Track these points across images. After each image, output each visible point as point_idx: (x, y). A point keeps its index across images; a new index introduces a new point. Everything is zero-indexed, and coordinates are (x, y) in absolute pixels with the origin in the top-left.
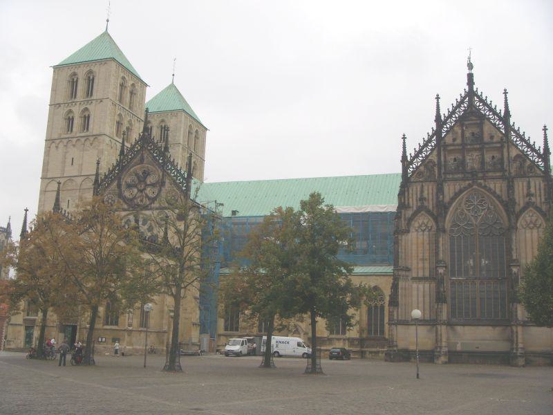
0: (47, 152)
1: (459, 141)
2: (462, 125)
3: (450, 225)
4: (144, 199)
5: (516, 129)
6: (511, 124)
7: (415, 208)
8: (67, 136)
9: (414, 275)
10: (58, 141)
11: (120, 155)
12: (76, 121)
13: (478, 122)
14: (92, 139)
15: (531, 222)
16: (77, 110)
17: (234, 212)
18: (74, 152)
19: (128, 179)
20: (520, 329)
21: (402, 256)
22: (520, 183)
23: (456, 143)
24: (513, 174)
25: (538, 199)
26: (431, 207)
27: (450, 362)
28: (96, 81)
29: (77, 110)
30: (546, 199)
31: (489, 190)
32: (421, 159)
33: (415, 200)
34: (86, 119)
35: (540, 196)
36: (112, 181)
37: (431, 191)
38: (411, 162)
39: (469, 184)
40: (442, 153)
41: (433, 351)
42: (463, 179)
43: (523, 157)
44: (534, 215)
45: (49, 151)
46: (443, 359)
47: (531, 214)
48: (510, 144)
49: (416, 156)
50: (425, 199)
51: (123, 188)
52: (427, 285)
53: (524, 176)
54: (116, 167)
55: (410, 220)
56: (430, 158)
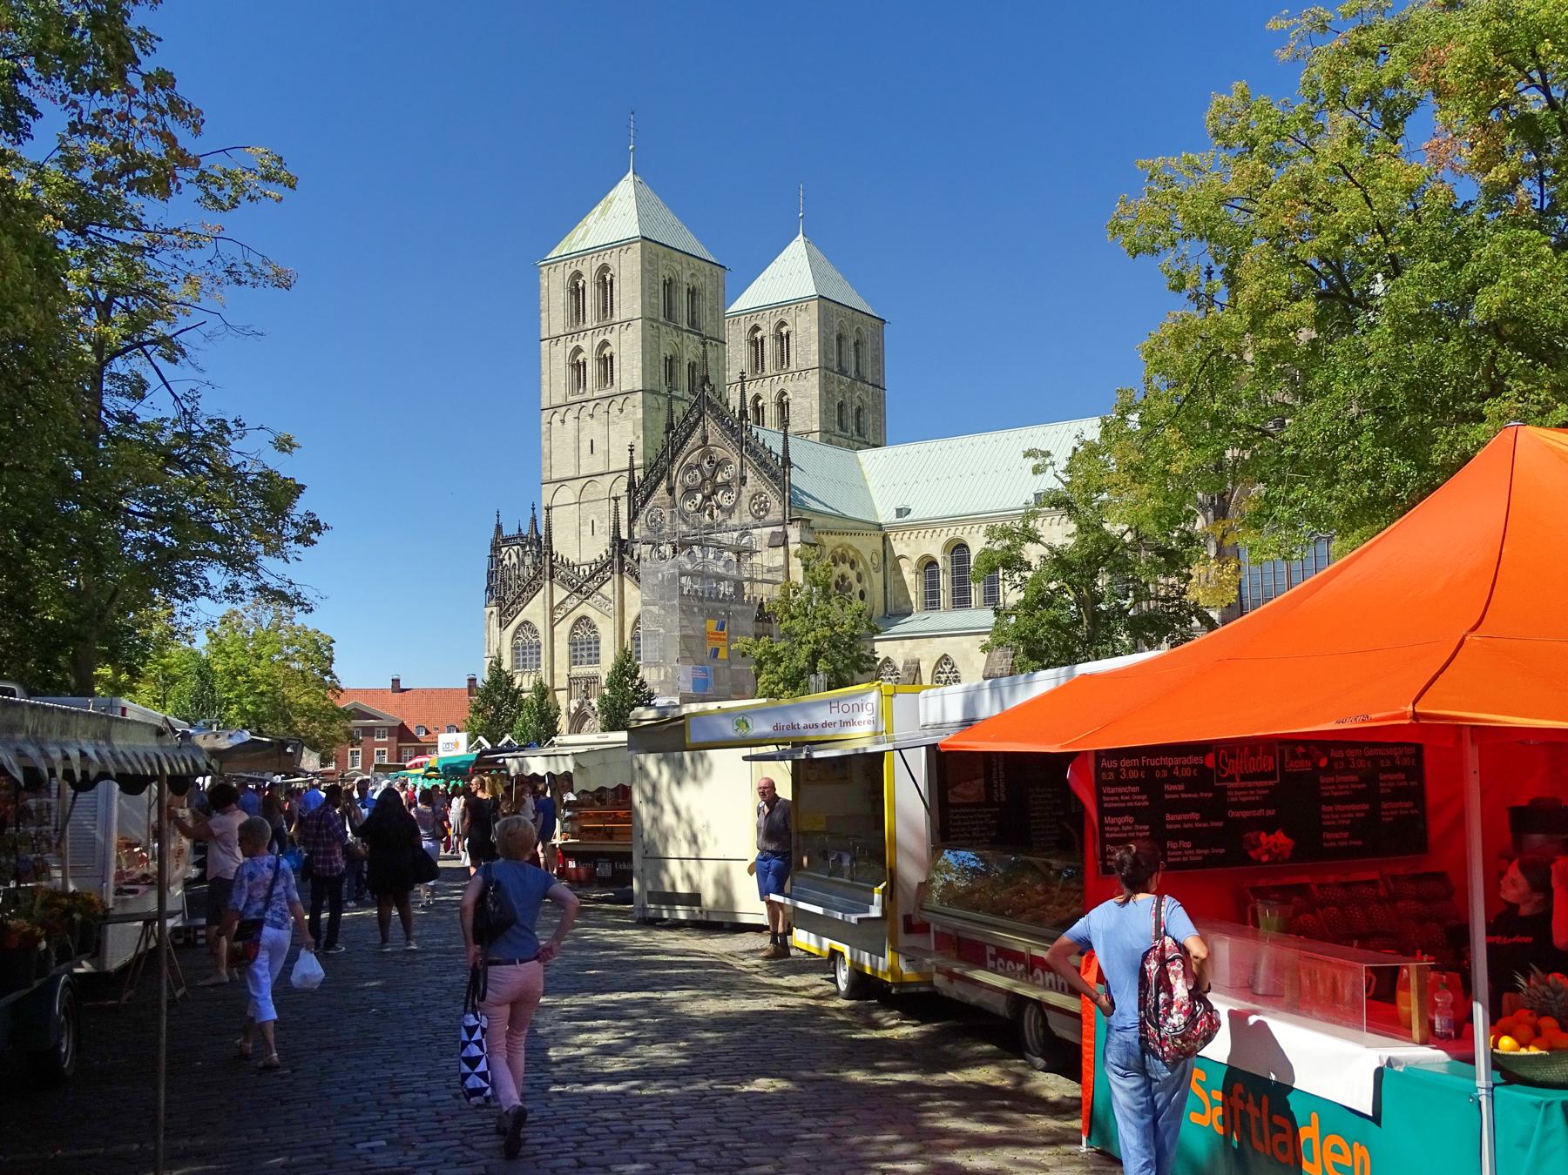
4: (715, 512)
10: (564, 409)
11: (667, 432)
12: (589, 369)
14: (620, 399)
17: (901, 512)
18: (593, 429)
28: (616, 285)
29: (588, 344)
34: (606, 363)
36: (658, 482)
51: (678, 493)
54: (662, 456)
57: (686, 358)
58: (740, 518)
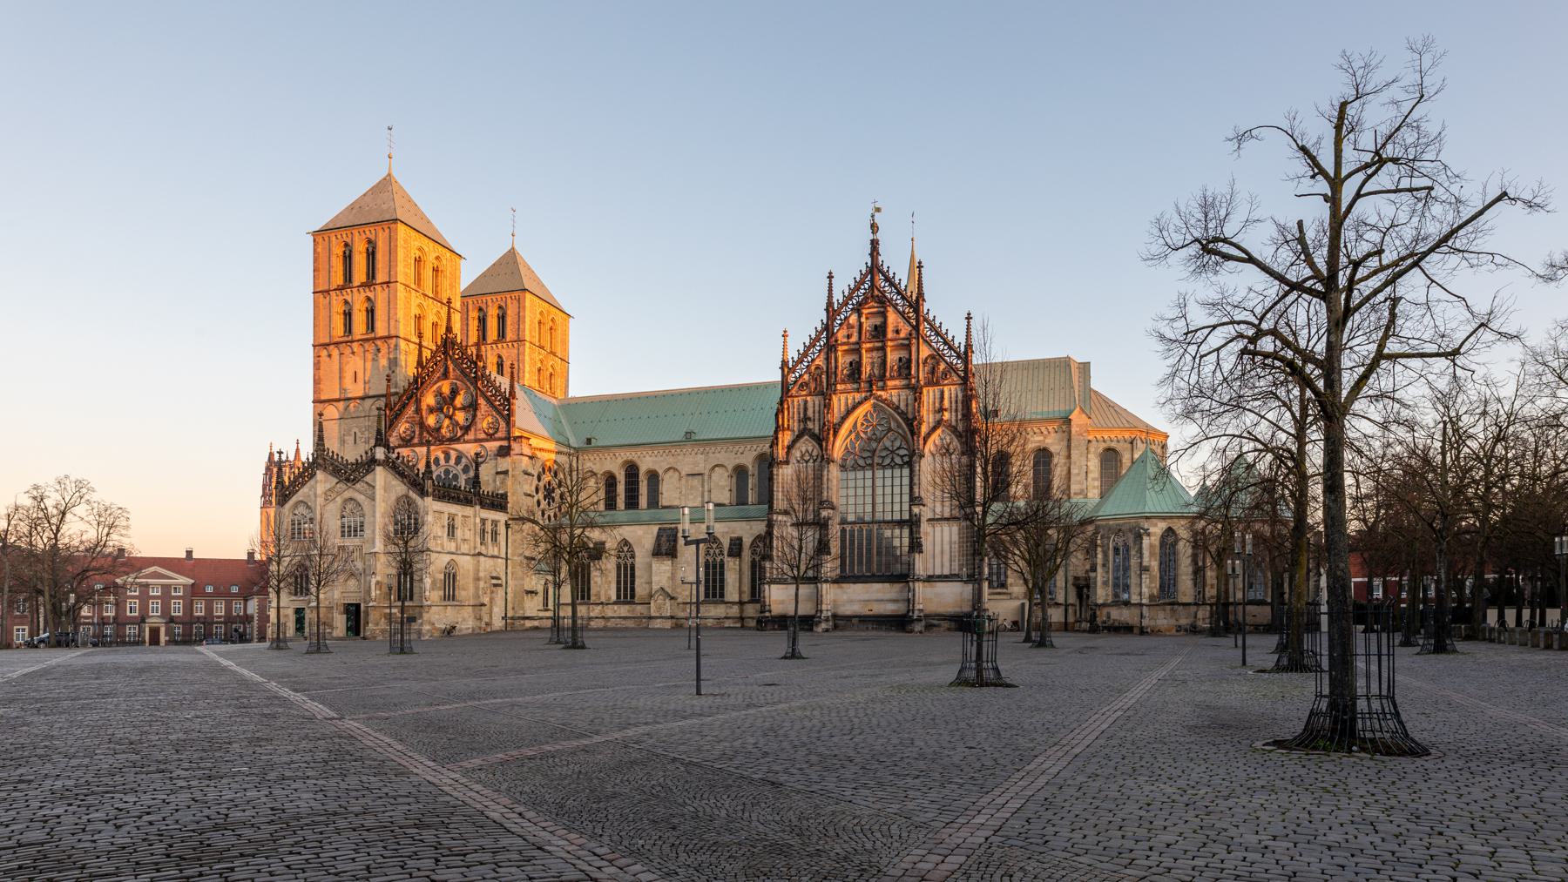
0: (317, 366)
1: (854, 339)
2: (860, 317)
5: (931, 318)
6: (925, 311)
7: (796, 433)
8: (346, 339)
10: (332, 347)
14: (379, 342)
15: (943, 446)
16: (358, 301)
19: (429, 400)
20: (919, 587)
24: (922, 383)
25: (953, 414)
26: (817, 431)
27: (836, 627)
29: (358, 301)
30: (963, 415)
34: (371, 312)
35: (956, 411)
37: (817, 408)
38: (792, 370)
41: (813, 617)
42: (858, 390)
43: (937, 357)
45: (319, 362)
46: (824, 626)
48: (921, 340)
49: (800, 361)
50: (809, 419)
53: (937, 384)
55: (790, 448)
56: (817, 362)
57: (431, 318)
58: (475, 434)
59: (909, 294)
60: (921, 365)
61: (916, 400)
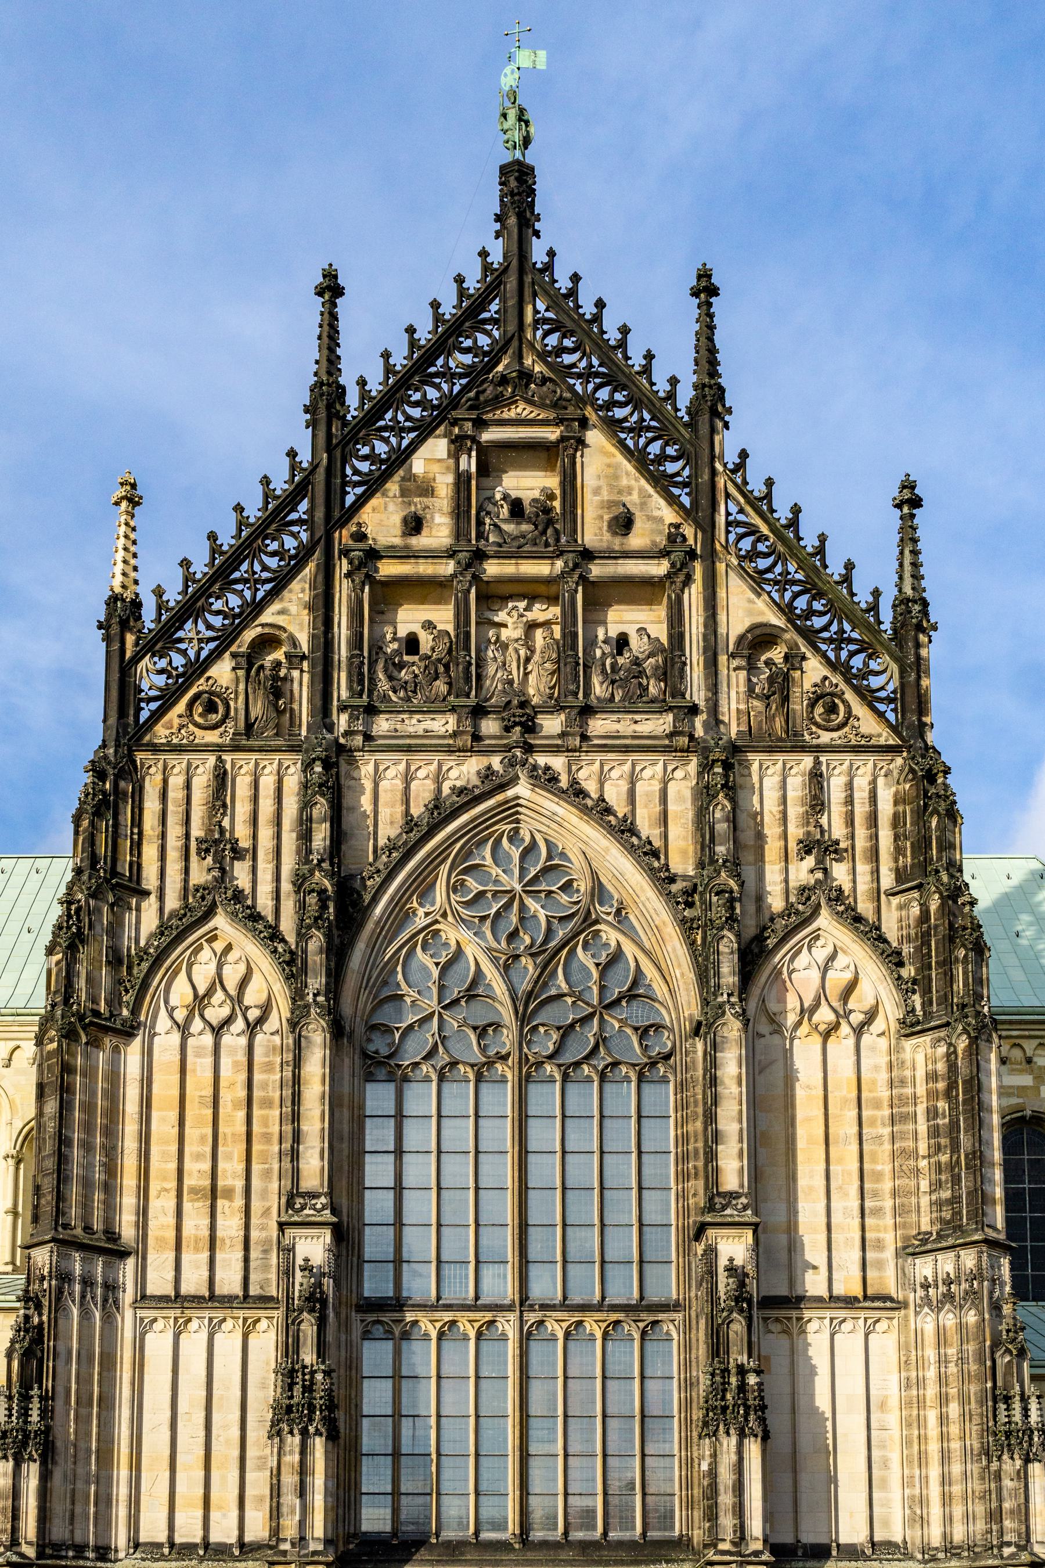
3: (365, 1001)
5: (757, 487)
7: (172, 903)
9: (159, 1282)
13: (552, 434)
21: (88, 1167)
22: (771, 783)
23: (421, 541)
25: (863, 869)
30: (900, 876)
31: (601, 811)
32: (217, 621)
33: (173, 855)
37: (266, 807)
39: (488, 773)
40: (343, 590)
44: (841, 960)
47: (821, 953)
52: (228, 1342)
56: (268, 616)
59: (662, 387)
60: (723, 659)
61: (704, 796)
